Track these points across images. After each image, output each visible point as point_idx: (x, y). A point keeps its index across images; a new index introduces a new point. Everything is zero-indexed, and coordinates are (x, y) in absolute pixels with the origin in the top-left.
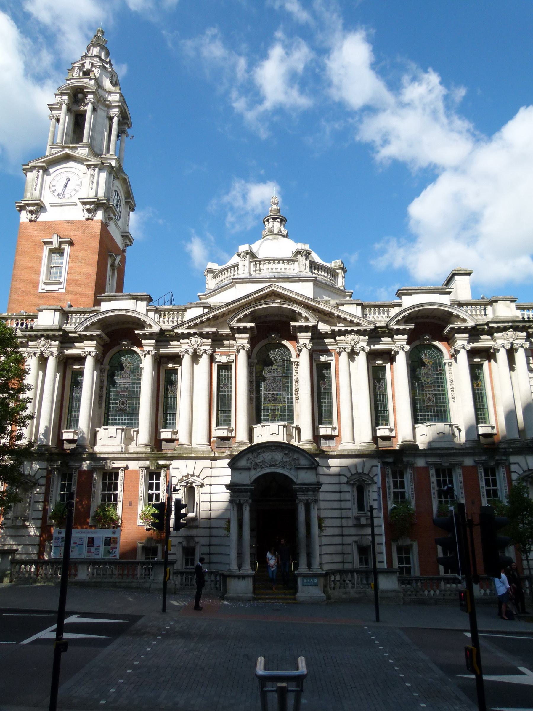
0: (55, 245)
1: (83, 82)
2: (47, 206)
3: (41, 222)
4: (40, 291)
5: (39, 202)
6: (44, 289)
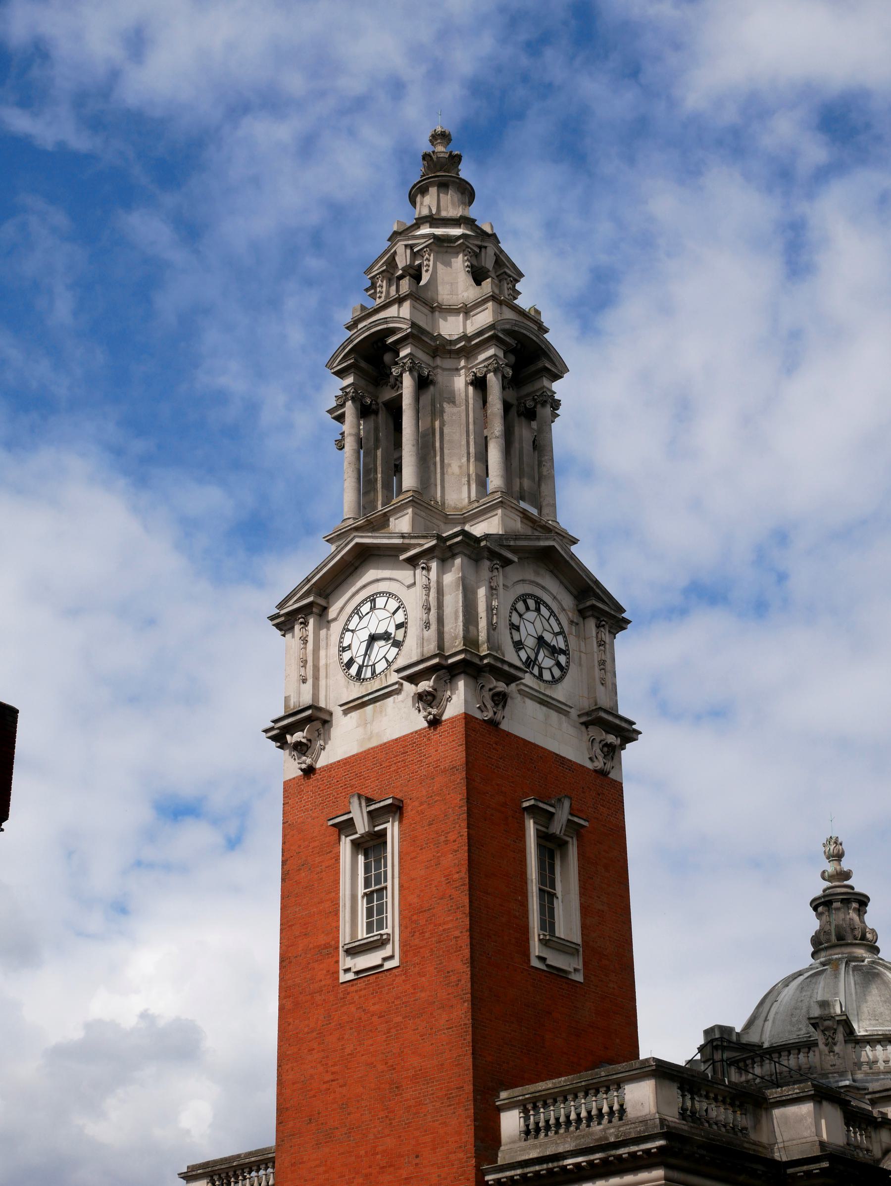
0: (362, 826)
1: (385, 320)
2: (338, 712)
3: (329, 768)
4: (344, 977)
5: (309, 712)
6: (347, 970)
